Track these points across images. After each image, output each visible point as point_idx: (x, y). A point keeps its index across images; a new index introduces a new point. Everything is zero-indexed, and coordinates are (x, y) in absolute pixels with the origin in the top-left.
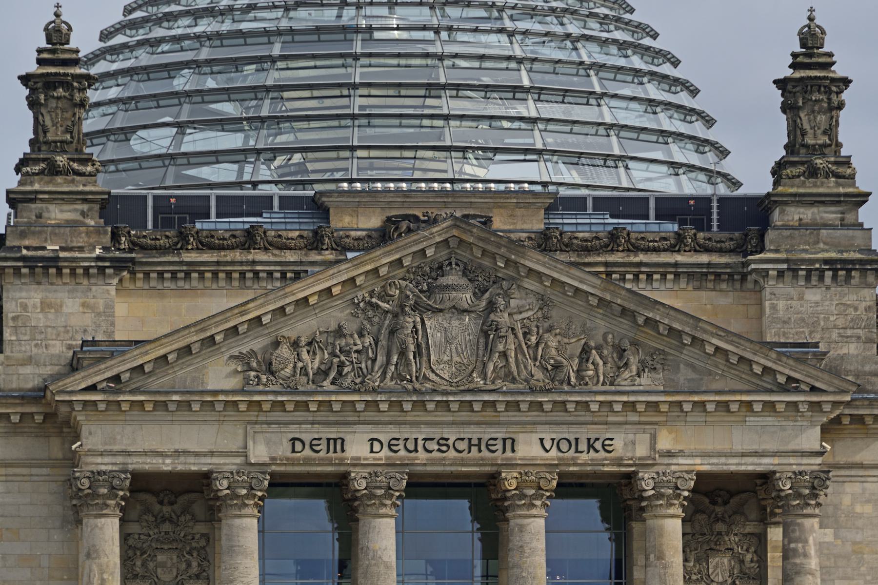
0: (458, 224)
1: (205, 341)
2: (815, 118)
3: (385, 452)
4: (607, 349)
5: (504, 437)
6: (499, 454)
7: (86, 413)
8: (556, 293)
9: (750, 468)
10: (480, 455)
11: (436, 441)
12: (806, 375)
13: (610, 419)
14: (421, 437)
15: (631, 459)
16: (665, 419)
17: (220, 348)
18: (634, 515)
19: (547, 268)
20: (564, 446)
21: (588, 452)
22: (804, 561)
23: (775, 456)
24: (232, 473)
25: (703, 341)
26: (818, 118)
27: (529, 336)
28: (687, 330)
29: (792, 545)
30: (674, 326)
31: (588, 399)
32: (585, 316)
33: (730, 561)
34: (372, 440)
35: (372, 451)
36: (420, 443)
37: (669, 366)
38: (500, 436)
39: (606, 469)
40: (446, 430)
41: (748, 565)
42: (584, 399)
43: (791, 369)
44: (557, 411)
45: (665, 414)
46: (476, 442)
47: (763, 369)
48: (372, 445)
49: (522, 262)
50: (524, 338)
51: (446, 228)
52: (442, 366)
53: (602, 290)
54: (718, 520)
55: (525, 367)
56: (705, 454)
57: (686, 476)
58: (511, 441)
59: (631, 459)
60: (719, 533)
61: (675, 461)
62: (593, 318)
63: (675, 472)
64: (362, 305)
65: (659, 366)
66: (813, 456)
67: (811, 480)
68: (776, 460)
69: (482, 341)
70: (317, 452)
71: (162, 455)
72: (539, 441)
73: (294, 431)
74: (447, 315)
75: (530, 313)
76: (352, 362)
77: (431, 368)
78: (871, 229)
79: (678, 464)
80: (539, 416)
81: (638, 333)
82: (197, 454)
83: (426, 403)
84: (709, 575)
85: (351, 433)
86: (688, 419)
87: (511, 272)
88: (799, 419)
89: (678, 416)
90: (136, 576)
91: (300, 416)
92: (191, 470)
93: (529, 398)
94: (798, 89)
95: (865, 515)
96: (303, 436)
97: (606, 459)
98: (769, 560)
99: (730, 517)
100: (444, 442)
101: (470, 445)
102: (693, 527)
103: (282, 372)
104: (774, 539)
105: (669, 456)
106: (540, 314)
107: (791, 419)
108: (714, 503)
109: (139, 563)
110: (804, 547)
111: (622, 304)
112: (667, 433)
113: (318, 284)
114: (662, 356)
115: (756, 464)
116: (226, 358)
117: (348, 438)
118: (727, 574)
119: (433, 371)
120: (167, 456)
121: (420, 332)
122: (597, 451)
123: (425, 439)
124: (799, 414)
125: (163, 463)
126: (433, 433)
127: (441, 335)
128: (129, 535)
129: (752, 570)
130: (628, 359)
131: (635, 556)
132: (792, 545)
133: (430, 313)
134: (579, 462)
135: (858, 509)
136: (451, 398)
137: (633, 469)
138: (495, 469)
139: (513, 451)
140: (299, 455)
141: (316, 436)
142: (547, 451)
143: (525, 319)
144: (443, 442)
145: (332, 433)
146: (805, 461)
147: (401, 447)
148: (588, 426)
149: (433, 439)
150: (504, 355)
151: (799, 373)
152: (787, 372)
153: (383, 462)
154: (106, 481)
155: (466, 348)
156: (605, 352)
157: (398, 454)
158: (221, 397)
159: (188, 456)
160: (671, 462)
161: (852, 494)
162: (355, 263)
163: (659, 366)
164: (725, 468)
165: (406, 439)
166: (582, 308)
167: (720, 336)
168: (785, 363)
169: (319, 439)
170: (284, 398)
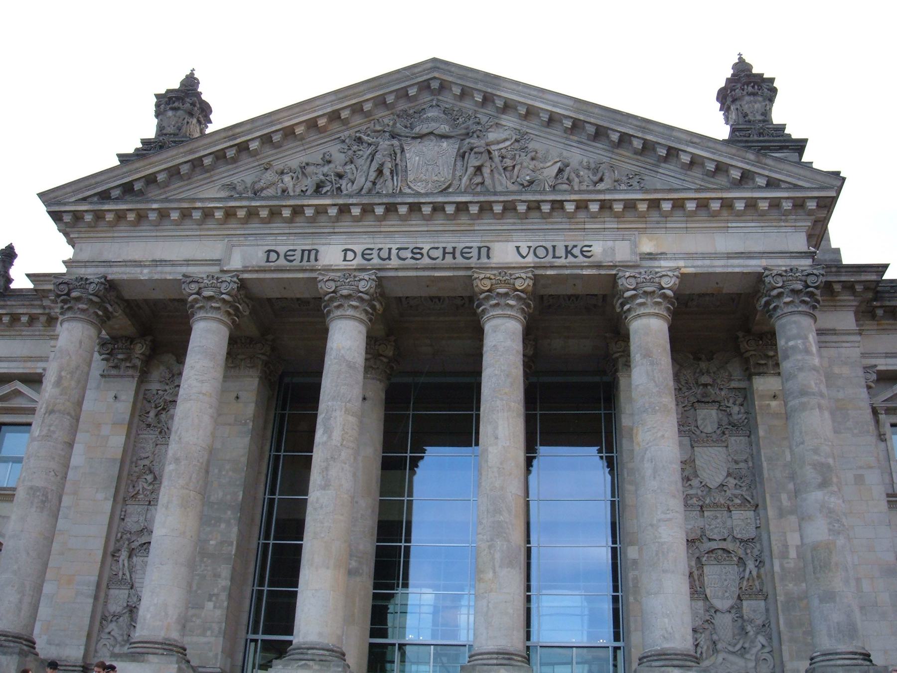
0: (438, 65)
2: (753, 106)
7: (80, 229)
8: (532, 125)
9: (737, 270)
10: (454, 261)
11: (410, 250)
12: (787, 175)
13: (587, 226)
14: (394, 247)
15: (611, 262)
16: (644, 226)
17: (211, 176)
18: (620, 368)
19: (524, 97)
20: (541, 252)
21: (566, 258)
22: (807, 357)
23: (761, 258)
26: (756, 106)
29: (791, 343)
30: (648, 138)
31: (564, 199)
32: (562, 146)
33: (717, 414)
34: (346, 250)
35: (345, 260)
36: (394, 252)
37: (645, 184)
39: (585, 273)
40: (420, 240)
41: (735, 417)
43: (770, 170)
45: (644, 219)
46: (451, 250)
47: (742, 174)
48: (345, 254)
49: (498, 93)
51: (428, 70)
52: (419, 184)
53: (575, 112)
54: (703, 374)
55: (501, 184)
56: (689, 256)
57: (670, 274)
58: (487, 249)
59: (611, 262)
60: (705, 385)
61: (656, 263)
62: (569, 148)
63: (656, 273)
64: (347, 141)
65: (635, 184)
66: (802, 257)
67: (804, 278)
68: (764, 262)
69: (459, 163)
70: (291, 261)
71: (141, 266)
72: (515, 249)
73: (269, 243)
74: (426, 142)
75: (508, 143)
76: (332, 183)
77: (408, 185)
78: (812, 162)
79: (660, 267)
80: (514, 224)
81: (613, 156)
82: (173, 263)
83: (398, 206)
84: (697, 427)
85: (326, 244)
86: (668, 225)
87: (490, 110)
88: (783, 224)
90: (149, 426)
91: (277, 227)
92: (166, 280)
94: (736, 87)
95: (843, 375)
96: (278, 249)
97: (584, 262)
98: (757, 407)
99: (714, 373)
100: (418, 251)
101: (444, 253)
103: (265, 192)
104: (761, 388)
105: (651, 259)
107: (774, 224)
109: (152, 414)
110: (804, 343)
111: (595, 122)
112: (648, 241)
113: (304, 115)
115: (743, 266)
116: (218, 187)
117: (322, 249)
118: (716, 426)
119: (410, 188)
120: (145, 266)
121: (398, 155)
122: (576, 257)
123: (399, 249)
124: (783, 218)
125: (141, 273)
126: (408, 243)
127: (419, 159)
128: (149, 390)
129: (741, 421)
130: (603, 175)
131: (623, 405)
132: (791, 343)
134: (556, 264)
135: (836, 370)
136: (423, 200)
137: (614, 272)
138: (469, 273)
139: (488, 257)
140: (272, 264)
141: (292, 248)
142: (524, 257)
143: (502, 149)
144: (417, 252)
146: (795, 262)
147: (375, 255)
148: (565, 233)
150: (479, 169)
151: (780, 173)
152: (766, 173)
153: (354, 267)
154: (83, 288)
156: (582, 173)
157: (371, 262)
159: (166, 265)
160: (653, 265)
161: (829, 358)
163: (635, 184)
164: (711, 270)
165: (380, 249)
166: (557, 139)
167: (695, 143)
168: (765, 164)
169: (294, 250)
170: (258, 204)
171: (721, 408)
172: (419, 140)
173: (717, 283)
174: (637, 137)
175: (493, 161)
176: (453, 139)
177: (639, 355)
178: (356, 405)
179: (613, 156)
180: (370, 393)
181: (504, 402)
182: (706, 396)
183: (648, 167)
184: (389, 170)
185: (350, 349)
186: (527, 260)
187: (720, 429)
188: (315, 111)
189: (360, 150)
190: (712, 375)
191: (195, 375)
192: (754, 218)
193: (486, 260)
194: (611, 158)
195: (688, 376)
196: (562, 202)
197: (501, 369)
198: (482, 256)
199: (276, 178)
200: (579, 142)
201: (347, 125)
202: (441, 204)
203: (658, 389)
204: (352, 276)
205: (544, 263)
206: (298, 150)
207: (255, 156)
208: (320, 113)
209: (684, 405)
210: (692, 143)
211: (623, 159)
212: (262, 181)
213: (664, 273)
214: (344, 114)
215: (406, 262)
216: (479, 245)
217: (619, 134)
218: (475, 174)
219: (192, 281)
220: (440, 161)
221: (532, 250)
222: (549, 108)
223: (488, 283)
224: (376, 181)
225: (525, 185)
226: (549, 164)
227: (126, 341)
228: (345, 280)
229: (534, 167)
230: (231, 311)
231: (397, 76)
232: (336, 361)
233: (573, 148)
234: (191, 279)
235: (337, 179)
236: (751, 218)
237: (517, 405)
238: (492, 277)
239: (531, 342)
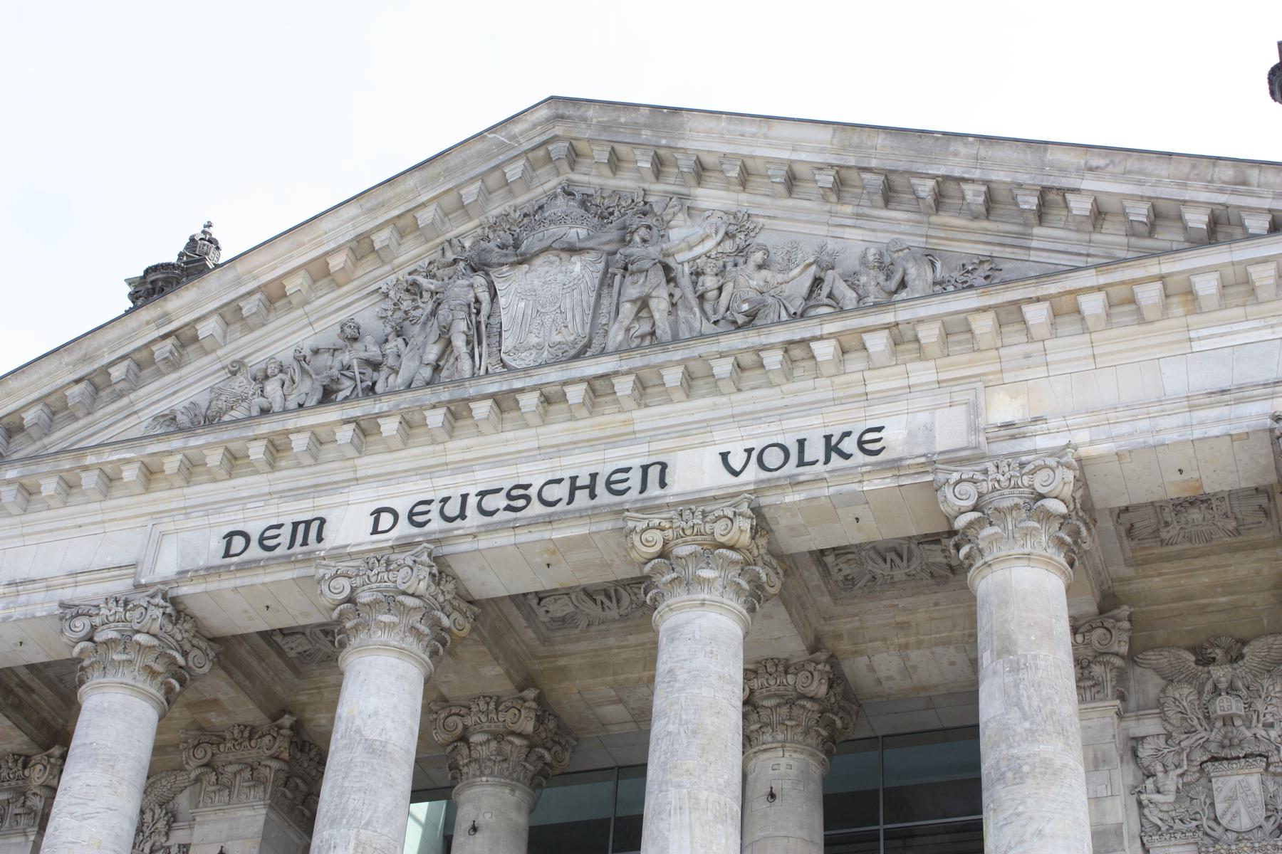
0: (562, 110)
1: (103, 394)
3: (404, 528)
4: (868, 275)
5: (645, 463)
6: (633, 494)
8: (759, 199)
10: (593, 503)
11: (504, 493)
14: (473, 491)
20: (773, 458)
21: (827, 461)
24: (97, 606)
25: (1063, 191)
27: (701, 278)
28: (1023, 178)
30: (994, 178)
31: (807, 335)
36: (472, 501)
38: (636, 463)
42: (797, 337)
44: (753, 388)
46: (587, 481)
49: (680, 145)
50: (695, 284)
51: (541, 123)
57: (1052, 462)
58: (659, 467)
59: (925, 455)
60: (1228, 720)
61: (1027, 445)
64: (392, 294)
72: (720, 458)
74: (540, 269)
75: (709, 244)
76: (353, 379)
79: (1035, 451)
80: (715, 407)
84: (1216, 819)
85: (339, 505)
89: (1027, 356)
93: (677, 356)
97: (865, 465)
100: (521, 492)
101: (573, 489)
102: (1165, 719)
105: (1013, 437)
106: (728, 246)
108: (1205, 661)
114: (987, 266)
115: (1229, 420)
116: (145, 424)
118: (1261, 813)
122: (847, 456)
123: (482, 494)
130: (905, 273)
133: (505, 268)
134: (802, 478)
136: (518, 384)
139: (663, 484)
141: (274, 523)
145: (301, 510)
149: (498, 491)
150: (643, 304)
155: (574, 317)
158: (90, 460)
160: (1017, 449)
162: (369, 205)
165: (445, 500)
171: (1271, 769)
172: (525, 267)
173: (1181, 471)
174: (973, 181)
175: (676, 286)
176: (593, 253)
177: (989, 652)
178: (385, 831)
179: (931, 232)
180: (488, 816)
181: (685, 791)
182: (1231, 746)
183: (1008, 241)
184: (463, 337)
185: (376, 713)
186: (743, 477)
187: (1272, 820)
188: (321, 244)
189: (416, 308)
190: (1244, 693)
191: (69, 805)
192: (1250, 309)
193: (659, 492)
194: (927, 236)
195: (1185, 703)
196: (804, 342)
197: (681, 720)
198: (649, 484)
199: (252, 388)
200: (857, 215)
201: (390, 262)
202: (557, 388)
203: (1027, 725)
204: (382, 562)
205: (778, 479)
206: (298, 326)
207: (214, 351)
208: (332, 245)
209: (1179, 771)
210: (1091, 169)
211: (951, 234)
212: (223, 398)
213: (1040, 462)
214: (380, 239)
215: (496, 518)
216: (646, 461)
217: (932, 183)
218: (637, 317)
219: (78, 615)
220: (568, 301)
221: (754, 455)
222: (786, 155)
223: (657, 536)
224: (441, 363)
225: (740, 322)
226: (796, 271)
227: (16, 761)
228: (369, 572)
229: (762, 283)
230: (158, 667)
231: (479, 146)
232: (345, 742)
233: (848, 230)
234: (74, 611)
235: (369, 371)
236: (1240, 311)
237: (715, 795)
238: (666, 524)
239: (820, 667)
